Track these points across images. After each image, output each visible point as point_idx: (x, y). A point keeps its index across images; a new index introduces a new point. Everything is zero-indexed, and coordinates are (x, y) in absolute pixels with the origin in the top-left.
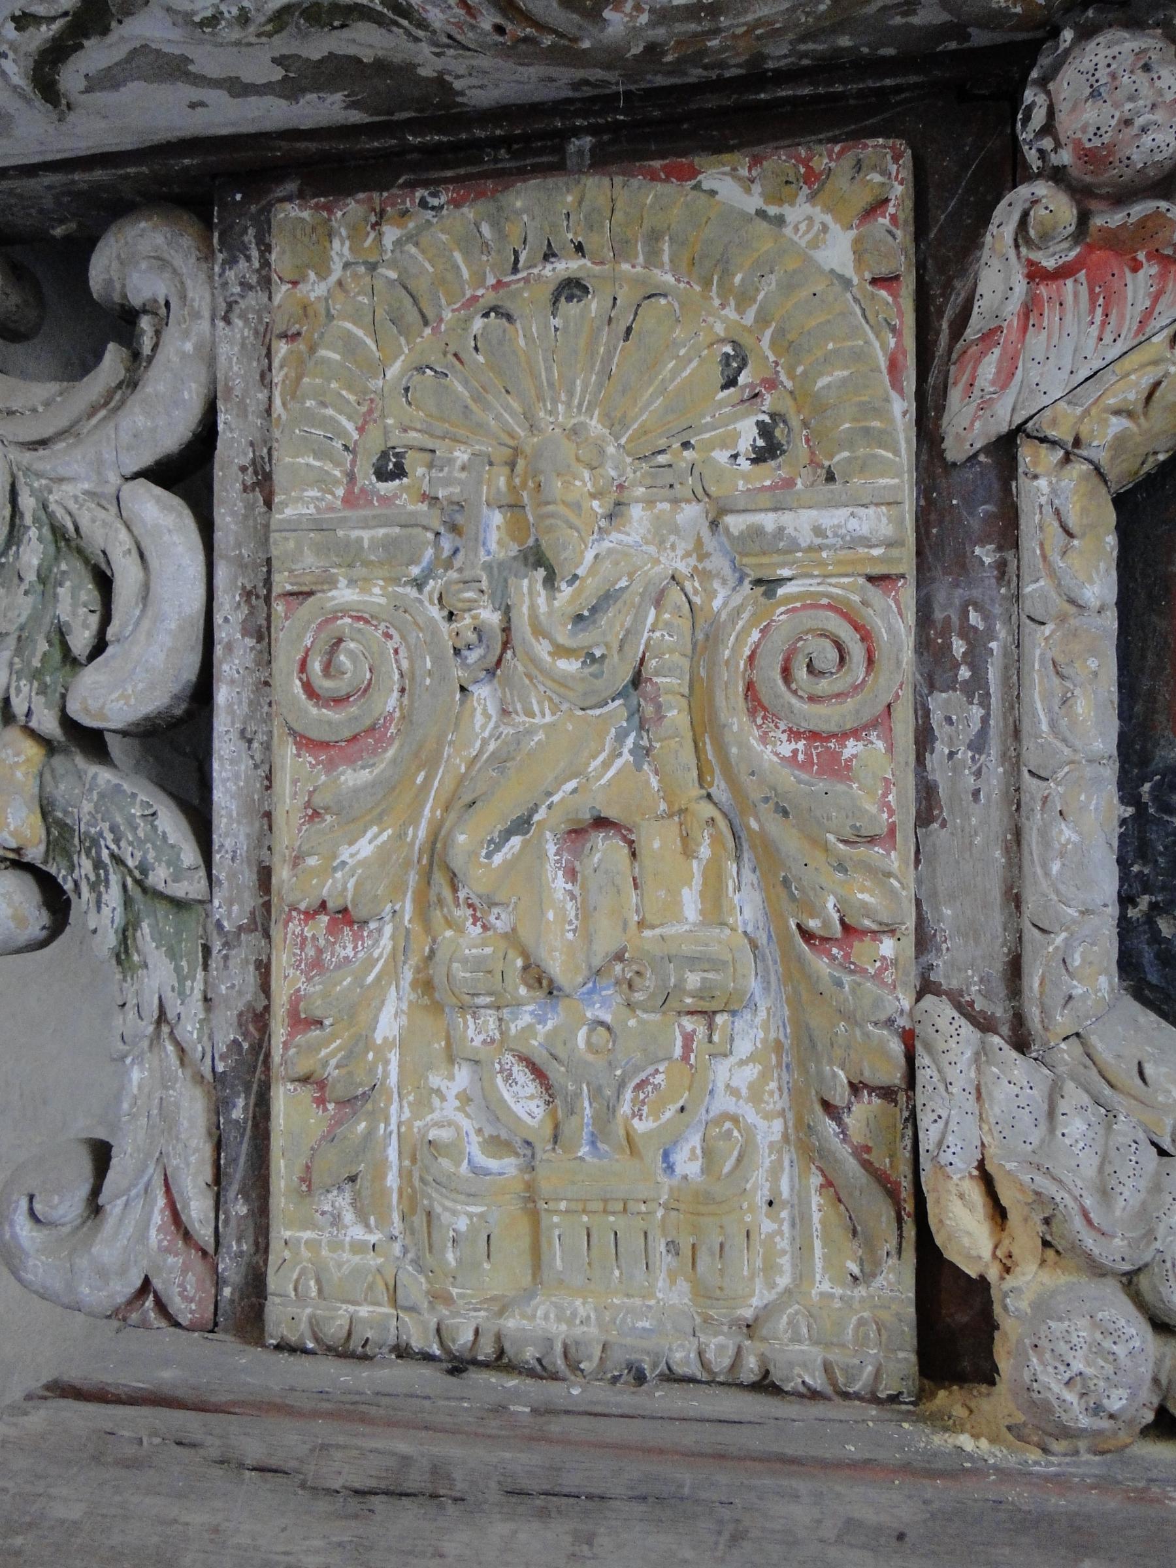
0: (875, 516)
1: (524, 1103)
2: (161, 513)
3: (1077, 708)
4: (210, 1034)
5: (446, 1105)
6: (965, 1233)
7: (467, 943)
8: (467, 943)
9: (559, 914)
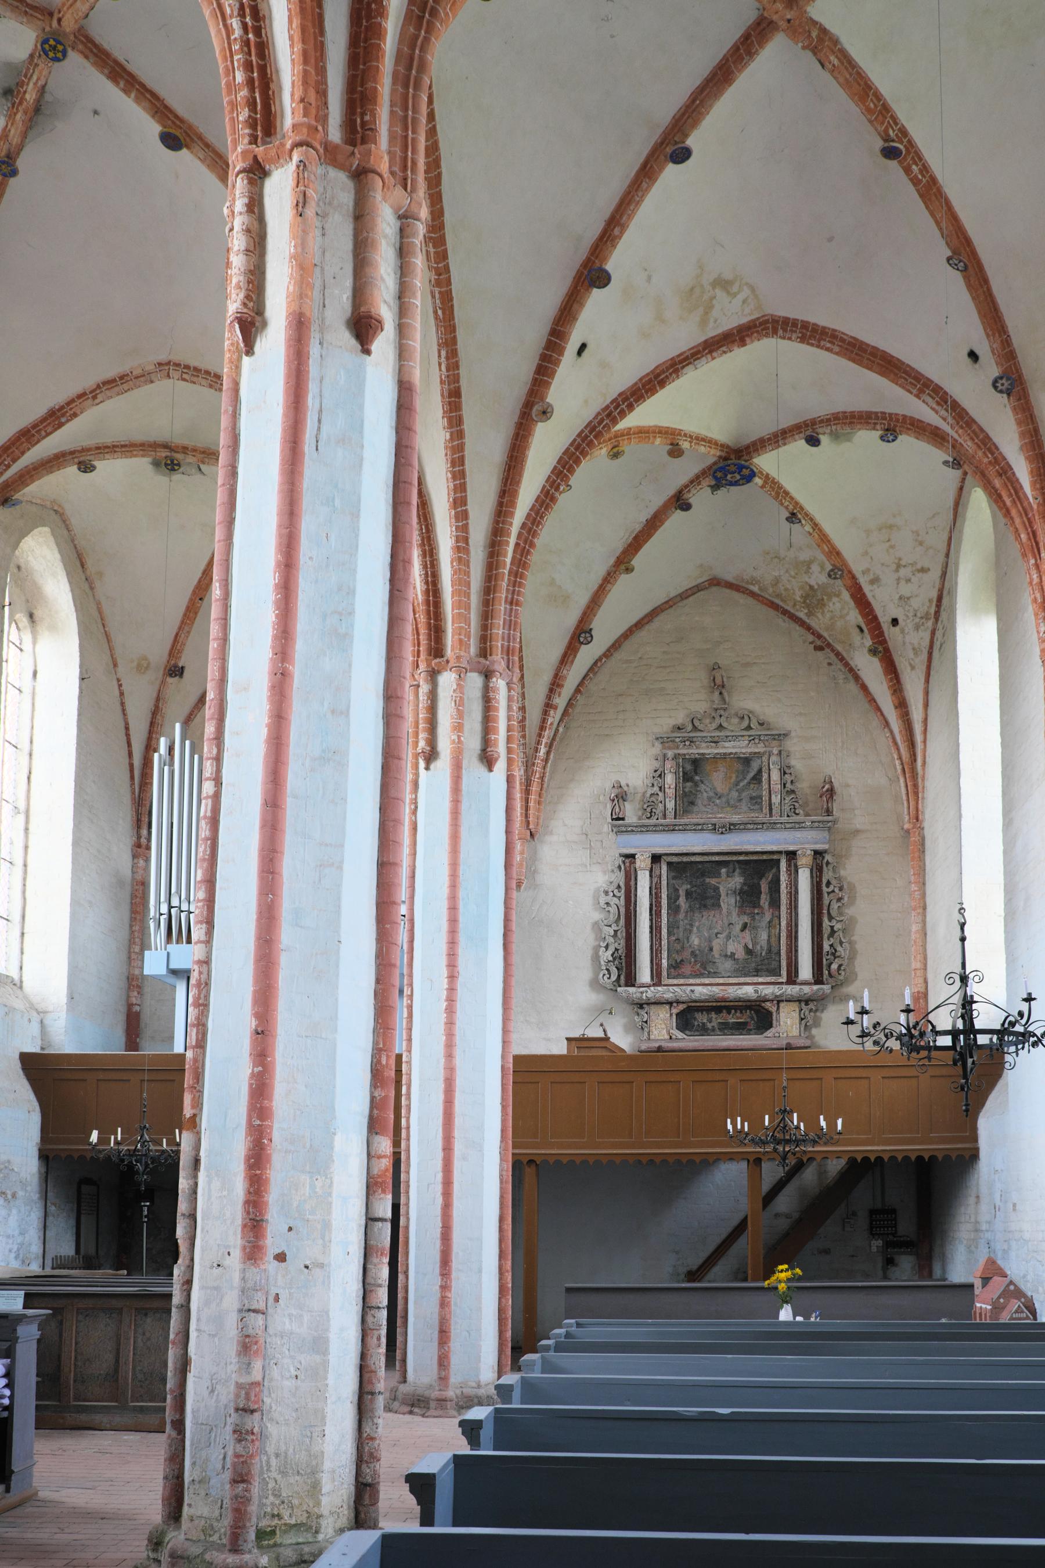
3: (674, 1020)
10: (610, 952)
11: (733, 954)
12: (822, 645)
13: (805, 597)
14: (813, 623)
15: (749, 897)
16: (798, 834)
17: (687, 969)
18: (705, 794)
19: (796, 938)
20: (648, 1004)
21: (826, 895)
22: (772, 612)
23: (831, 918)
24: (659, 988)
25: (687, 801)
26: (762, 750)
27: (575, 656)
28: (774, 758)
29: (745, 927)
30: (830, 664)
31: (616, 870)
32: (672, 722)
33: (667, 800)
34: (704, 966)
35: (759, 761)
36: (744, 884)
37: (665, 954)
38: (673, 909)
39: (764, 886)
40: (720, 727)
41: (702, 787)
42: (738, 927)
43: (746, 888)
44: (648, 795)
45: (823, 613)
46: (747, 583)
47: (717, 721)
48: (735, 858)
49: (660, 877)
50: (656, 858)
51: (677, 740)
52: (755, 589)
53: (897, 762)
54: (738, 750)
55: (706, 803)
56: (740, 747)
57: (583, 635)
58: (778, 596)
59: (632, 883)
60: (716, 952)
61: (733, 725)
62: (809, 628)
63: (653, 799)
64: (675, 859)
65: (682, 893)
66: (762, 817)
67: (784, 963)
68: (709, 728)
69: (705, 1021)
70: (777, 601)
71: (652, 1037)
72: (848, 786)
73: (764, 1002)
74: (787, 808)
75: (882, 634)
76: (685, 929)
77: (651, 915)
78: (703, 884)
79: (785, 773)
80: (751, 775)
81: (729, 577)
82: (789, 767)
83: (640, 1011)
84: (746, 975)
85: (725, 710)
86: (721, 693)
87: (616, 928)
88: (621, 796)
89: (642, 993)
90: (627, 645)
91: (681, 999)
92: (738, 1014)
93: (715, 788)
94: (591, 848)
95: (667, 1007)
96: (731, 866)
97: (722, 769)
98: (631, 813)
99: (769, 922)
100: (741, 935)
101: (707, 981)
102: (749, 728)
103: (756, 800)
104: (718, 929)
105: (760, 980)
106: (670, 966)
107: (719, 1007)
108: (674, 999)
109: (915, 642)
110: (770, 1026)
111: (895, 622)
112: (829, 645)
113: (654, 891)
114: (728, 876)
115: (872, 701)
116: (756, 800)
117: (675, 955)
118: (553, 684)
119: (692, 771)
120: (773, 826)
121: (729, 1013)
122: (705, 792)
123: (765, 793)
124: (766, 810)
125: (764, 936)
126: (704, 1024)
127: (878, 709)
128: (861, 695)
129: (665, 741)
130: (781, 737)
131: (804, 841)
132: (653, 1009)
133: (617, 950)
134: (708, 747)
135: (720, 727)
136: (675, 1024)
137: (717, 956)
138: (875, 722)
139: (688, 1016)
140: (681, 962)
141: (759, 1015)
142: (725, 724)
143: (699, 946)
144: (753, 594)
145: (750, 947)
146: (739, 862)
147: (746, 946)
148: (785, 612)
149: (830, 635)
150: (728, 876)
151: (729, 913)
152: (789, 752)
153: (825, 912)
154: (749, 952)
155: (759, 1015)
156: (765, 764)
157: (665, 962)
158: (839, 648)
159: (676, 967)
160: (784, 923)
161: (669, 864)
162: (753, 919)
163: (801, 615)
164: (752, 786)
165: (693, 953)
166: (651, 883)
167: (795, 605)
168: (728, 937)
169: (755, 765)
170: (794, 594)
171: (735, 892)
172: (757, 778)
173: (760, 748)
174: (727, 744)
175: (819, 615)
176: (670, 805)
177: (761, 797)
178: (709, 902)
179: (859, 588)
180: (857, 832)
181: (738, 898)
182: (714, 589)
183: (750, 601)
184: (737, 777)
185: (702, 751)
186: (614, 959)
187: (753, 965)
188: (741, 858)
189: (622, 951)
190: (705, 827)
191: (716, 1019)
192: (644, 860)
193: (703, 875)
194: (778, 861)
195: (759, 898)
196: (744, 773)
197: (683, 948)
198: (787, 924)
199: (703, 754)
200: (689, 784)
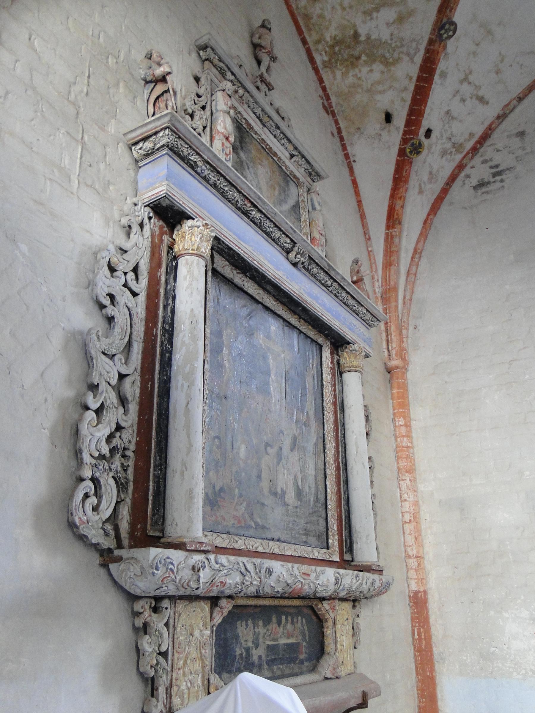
10: (105, 431)
13: (337, 42)
58: (307, 17)
133: (119, 428)
163: (318, 59)
167: (318, 42)
170: (327, 29)
175: (338, 74)
189: (129, 438)
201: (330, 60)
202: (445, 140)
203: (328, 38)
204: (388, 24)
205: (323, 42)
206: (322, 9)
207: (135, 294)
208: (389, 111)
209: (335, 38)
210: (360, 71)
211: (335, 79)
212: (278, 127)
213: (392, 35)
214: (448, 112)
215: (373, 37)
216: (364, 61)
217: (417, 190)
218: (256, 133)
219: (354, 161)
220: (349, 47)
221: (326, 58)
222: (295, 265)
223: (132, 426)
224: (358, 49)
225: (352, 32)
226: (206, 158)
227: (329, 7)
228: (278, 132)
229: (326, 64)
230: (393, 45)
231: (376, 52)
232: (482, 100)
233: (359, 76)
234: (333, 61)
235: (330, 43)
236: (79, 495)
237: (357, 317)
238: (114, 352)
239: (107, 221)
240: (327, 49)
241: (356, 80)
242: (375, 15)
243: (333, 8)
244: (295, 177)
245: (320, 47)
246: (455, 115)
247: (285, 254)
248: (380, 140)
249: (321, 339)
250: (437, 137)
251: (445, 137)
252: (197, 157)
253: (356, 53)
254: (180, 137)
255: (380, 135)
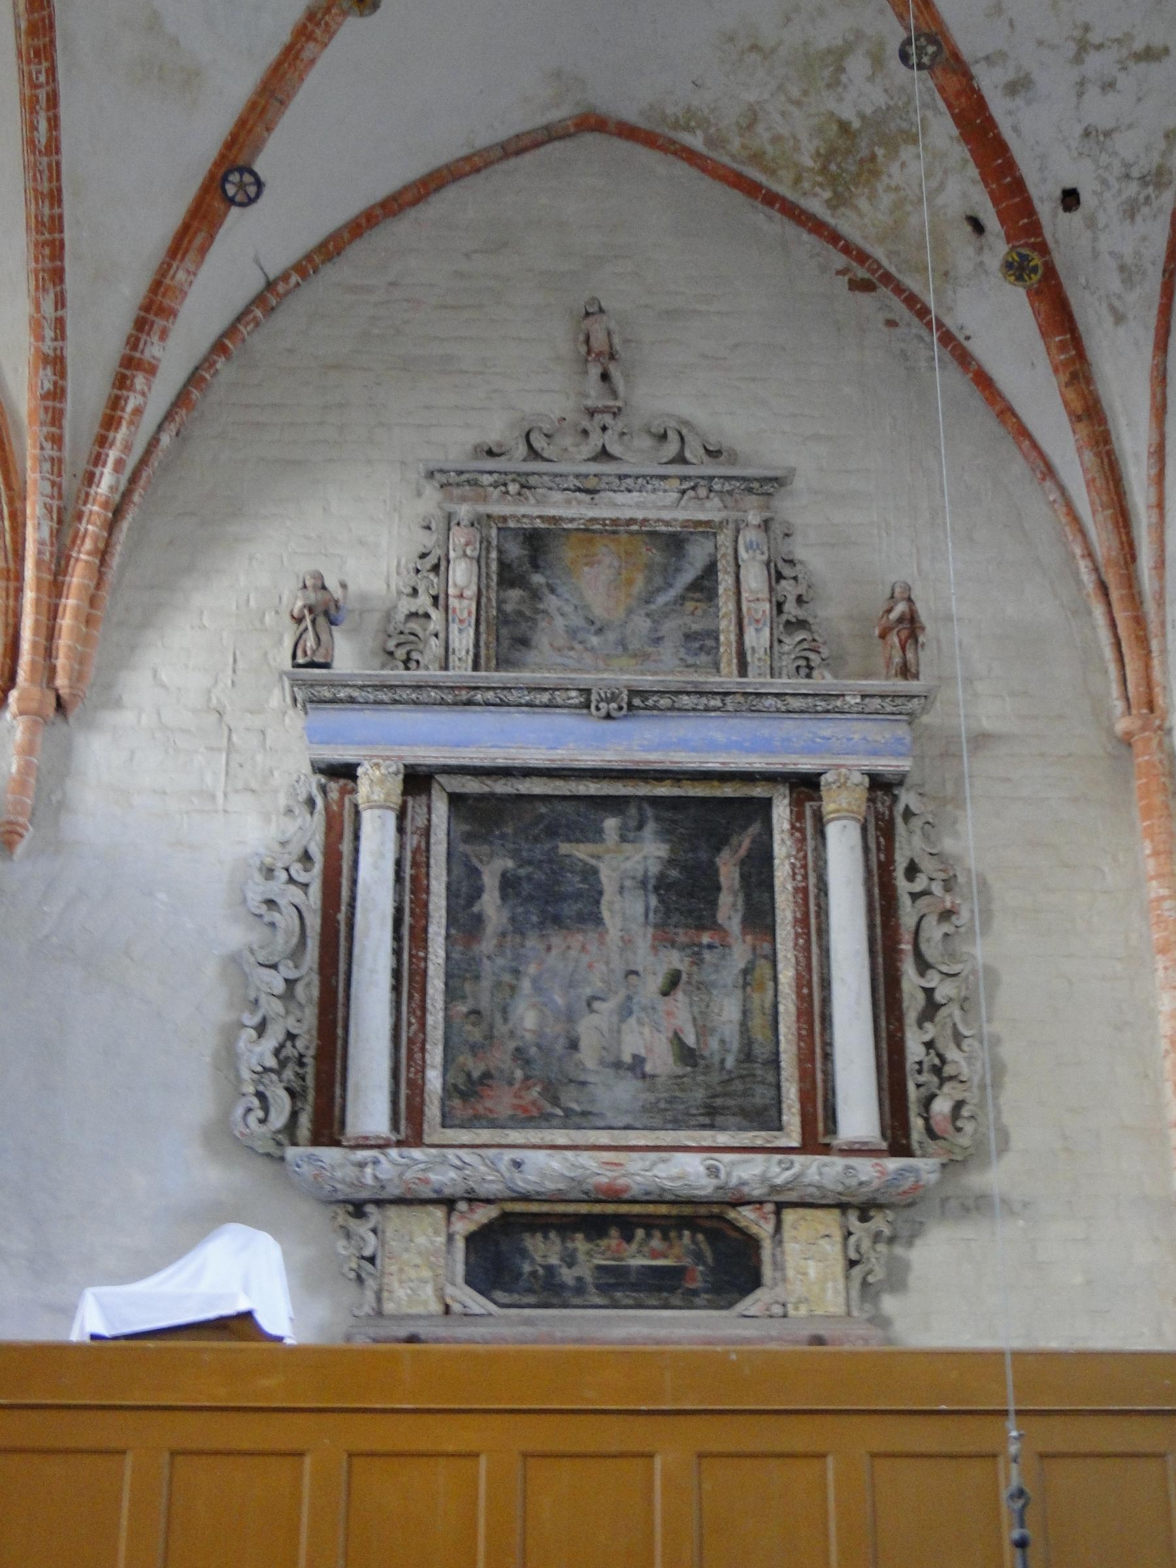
0: (441, 1239)
1: (409, 1292)
2: (371, 1235)
4: (375, 1287)
5: (401, 1293)
6: (449, 1301)
7: (404, 1277)
8: (404, 1277)
9: (412, 1273)
11: (638, 1061)
12: (868, 277)
13: (826, 158)
14: (845, 224)
15: (684, 900)
16: (827, 729)
17: (502, 1101)
18: (559, 622)
19: (827, 1020)
20: (379, 1203)
21: (905, 901)
22: (737, 196)
23: (923, 966)
24: (416, 1153)
25: (507, 634)
26: (716, 516)
27: (211, 237)
28: (749, 535)
29: (673, 982)
30: (891, 323)
31: (301, 810)
32: (472, 438)
33: (454, 628)
34: (551, 1093)
35: (709, 546)
36: (671, 862)
37: (435, 1055)
38: (465, 923)
39: (728, 872)
40: (604, 455)
41: (551, 602)
42: (653, 983)
43: (674, 873)
44: (400, 616)
45: (872, 197)
46: (676, 126)
47: (596, 441)
48: (644, 790)
49: (427, 832)
50: (417, 781)
51: (486, 479)
52: (695, 141)
53: (1083, 566)
54: (652, 515)
55: (561, 642)
56: (661, 507)
57: (235, 177)
58: (756, 158)
59: (346, 847)
60: (588, 1056)
61: (638, 456)
62: (834, 238)
63: (414, 625)
64: (472, 786)
65: (490, 880)
66: (727, 678)
67: (791, 1092)
68: (574, 459)
69: (554, 1260)
70: (754, 173)
71: (389, 1307)
72: (949, 618)
73: (736, 1204)
74: (787, 663)
75: (1035, 228)
76: (498, 985)
77: (397, 937)
78: (552, 858)
79: (780, 576)
80: (688, 576)
81: (630, 115)
82: (791, 562)
83: (353, 1224)
84: (677, 1124)
85: (616, 413)
86: (605, 377)
87: (292, 975)
88: (322, 612)
89: (361, 1165)
90: (357, 251)
91: (483, 1190)
92: (656, 1243)
93: (586, 607)
94: (230, 748)
95: (439, 1213)
96: (633, 811)
97: (607, 556)
98: (348, 657)
99: (746, 972)
100: (663, 1004)
101: (560, 1137)
102: (680, 459)
103: (701, 642)
104: (596, 985)
105: (723, 1139)
106: (449, 1090)
107: (602, 1217)
108: (459, 1191)
109: (1127, 250)
110: (752, 1281)
111: (1070, 199)
112: (887, 278)
113: (408, 872)
114: (623, 839)
115: (1006, 412)
116: (701, 642)
117: (465, 1059)
118: (147, 307)
119: (524, 562)
120: (752, 702)
121: (629, 1238)
122: (559, 614)
123: (727, 626)
124: (728, 662)
125: (728, 1011)
126: (550, 1269)
127: (1022, 432)
128: (975, 400)
129: (449, 480)
130: (769, 485)
131: (844, 751)
132: (395, 1218)
133: (291, 1037)
134: (568, 502)
135: (604, 455)
136: (460, 1269)
137: (590, 1064)
138: (1018, 466)
139: (504, 1247)
140: (478, 1089)
141: (720, 1252)
142: (615, 449)
143: (539, 1033)
144: (689, 156)
145: (690, 1040)
146: (654, 801)
147: (677, 1039)
148: (771, 199)
149: (890, 254)
150: (623, 839)
151: (627, 943)
152: (789, 525)
153: (906, 947)
154: (687, 1055)
155: (720, 1252)
156: (726, 548)
157: (434, 1079)
158: (912, 283)
159: (469, 1095)
160: (787, 975)
161: (456, 800)
162: (698, 961)
163: (816, 206)
164: (689, 606)
165: (520, 1054)
166: (401, 847)
167: (798, 180)
168: (625, 1011)
169: (697, 555)
170: (797, 149)
171: (643, 884)
172: (704, 586)
173: (712, 511)
174: (620, 498)
176: (463, 641)
177: (714, 635)
178: (569, 909)
179: (980, 105)
180: (981, 740)
181: (653, 901)
182: (589, 138)
183: (681, 169)
184: (649, 580)
185: (552, 512)
186: (283, 1064)
187: (700, 1095)
188: (663, 790)
189: (307, 1043)
190: (559, 697)
191: (589, 1256)
192: (382, 781)
193: (552, 832)
194: (767, 804)
195: (713, 904)
196: (668, 573)
197: (490, 1037)
198: (799, 977)
199: (554, 519)
200: (515, 594)
201: (835, 192)
202: (1117, 186)
203: (808, 162)
204: (871, 79)
205: (805, 175)
206: (769, 129)
207: (305, 886)
208: (969, 213)
209: (818, 154)
210: (890, 176)
211: (861, 215)
212: (621, 477)
213: (886, 91)
214: (1087, 134)
215: (868, 111)
216: (884, 156)
217: (1108, 320)
218: (572, 520)
219: (968, 338)
220: (848, 152)
221: (827, 194)
222: (608, 717)
223: (309, 1031)
224: (863, 144)
225: (835, 127)
226: (360, 683)
227: (777, 117)
228: (629, 481)
229: (834, 202)
230: (900, 104)
231: (889, 133)
232: (1150, 55)
233: (893, 185)
234: (840, 189)
235: (817, 166)
236: (239, 1111)
237: (849, 716)
238: (276, 959)
239: (267, 817)
240: (820, 179)
241: (893, 196)
242: (844, 78)
243: (783, 114)
244: (699, 523)
245: (806, 185)
246: (1109, 124)
247: (585, 711)
248: (986, 271)
249: (759, 790)
250: (1094, 192)
251: (1112, 181)
252: (347, 689)
253: (864, 153)
254: (312, 686)
255: (981, 263)
